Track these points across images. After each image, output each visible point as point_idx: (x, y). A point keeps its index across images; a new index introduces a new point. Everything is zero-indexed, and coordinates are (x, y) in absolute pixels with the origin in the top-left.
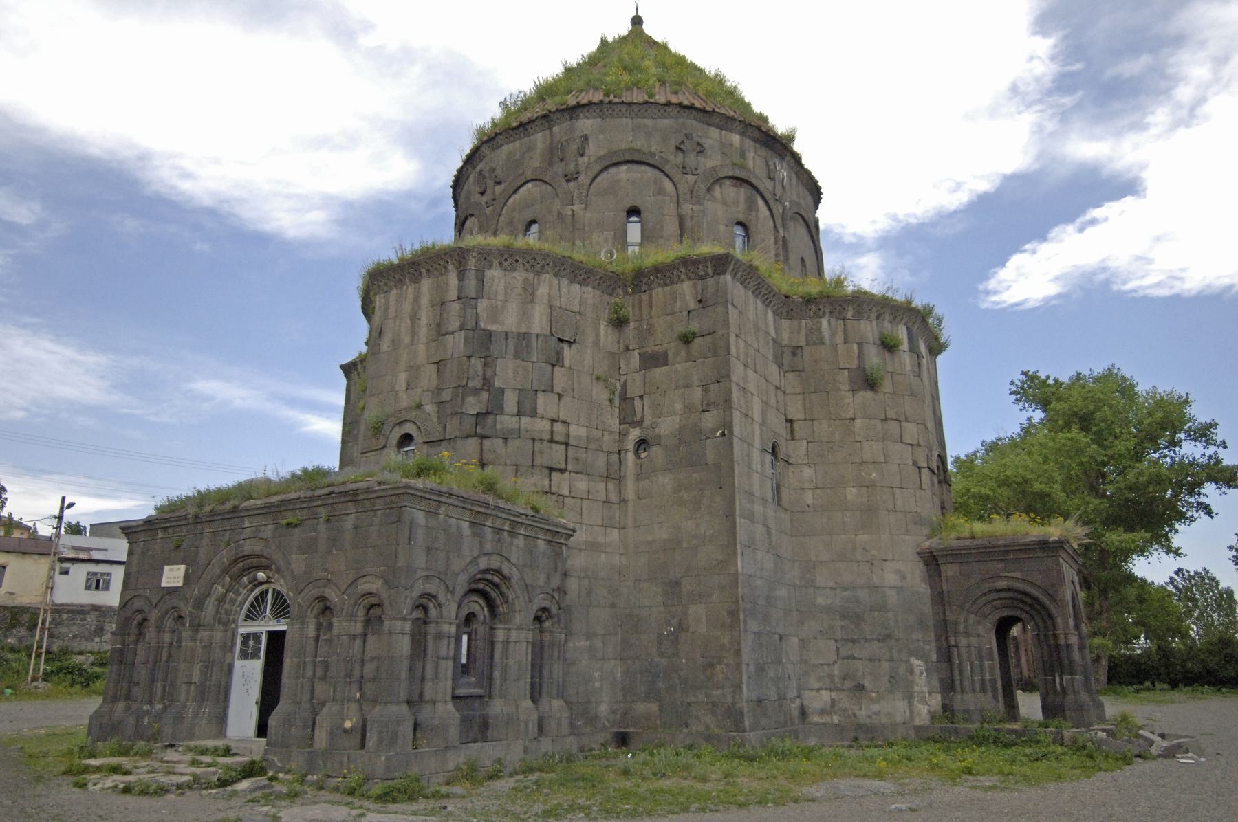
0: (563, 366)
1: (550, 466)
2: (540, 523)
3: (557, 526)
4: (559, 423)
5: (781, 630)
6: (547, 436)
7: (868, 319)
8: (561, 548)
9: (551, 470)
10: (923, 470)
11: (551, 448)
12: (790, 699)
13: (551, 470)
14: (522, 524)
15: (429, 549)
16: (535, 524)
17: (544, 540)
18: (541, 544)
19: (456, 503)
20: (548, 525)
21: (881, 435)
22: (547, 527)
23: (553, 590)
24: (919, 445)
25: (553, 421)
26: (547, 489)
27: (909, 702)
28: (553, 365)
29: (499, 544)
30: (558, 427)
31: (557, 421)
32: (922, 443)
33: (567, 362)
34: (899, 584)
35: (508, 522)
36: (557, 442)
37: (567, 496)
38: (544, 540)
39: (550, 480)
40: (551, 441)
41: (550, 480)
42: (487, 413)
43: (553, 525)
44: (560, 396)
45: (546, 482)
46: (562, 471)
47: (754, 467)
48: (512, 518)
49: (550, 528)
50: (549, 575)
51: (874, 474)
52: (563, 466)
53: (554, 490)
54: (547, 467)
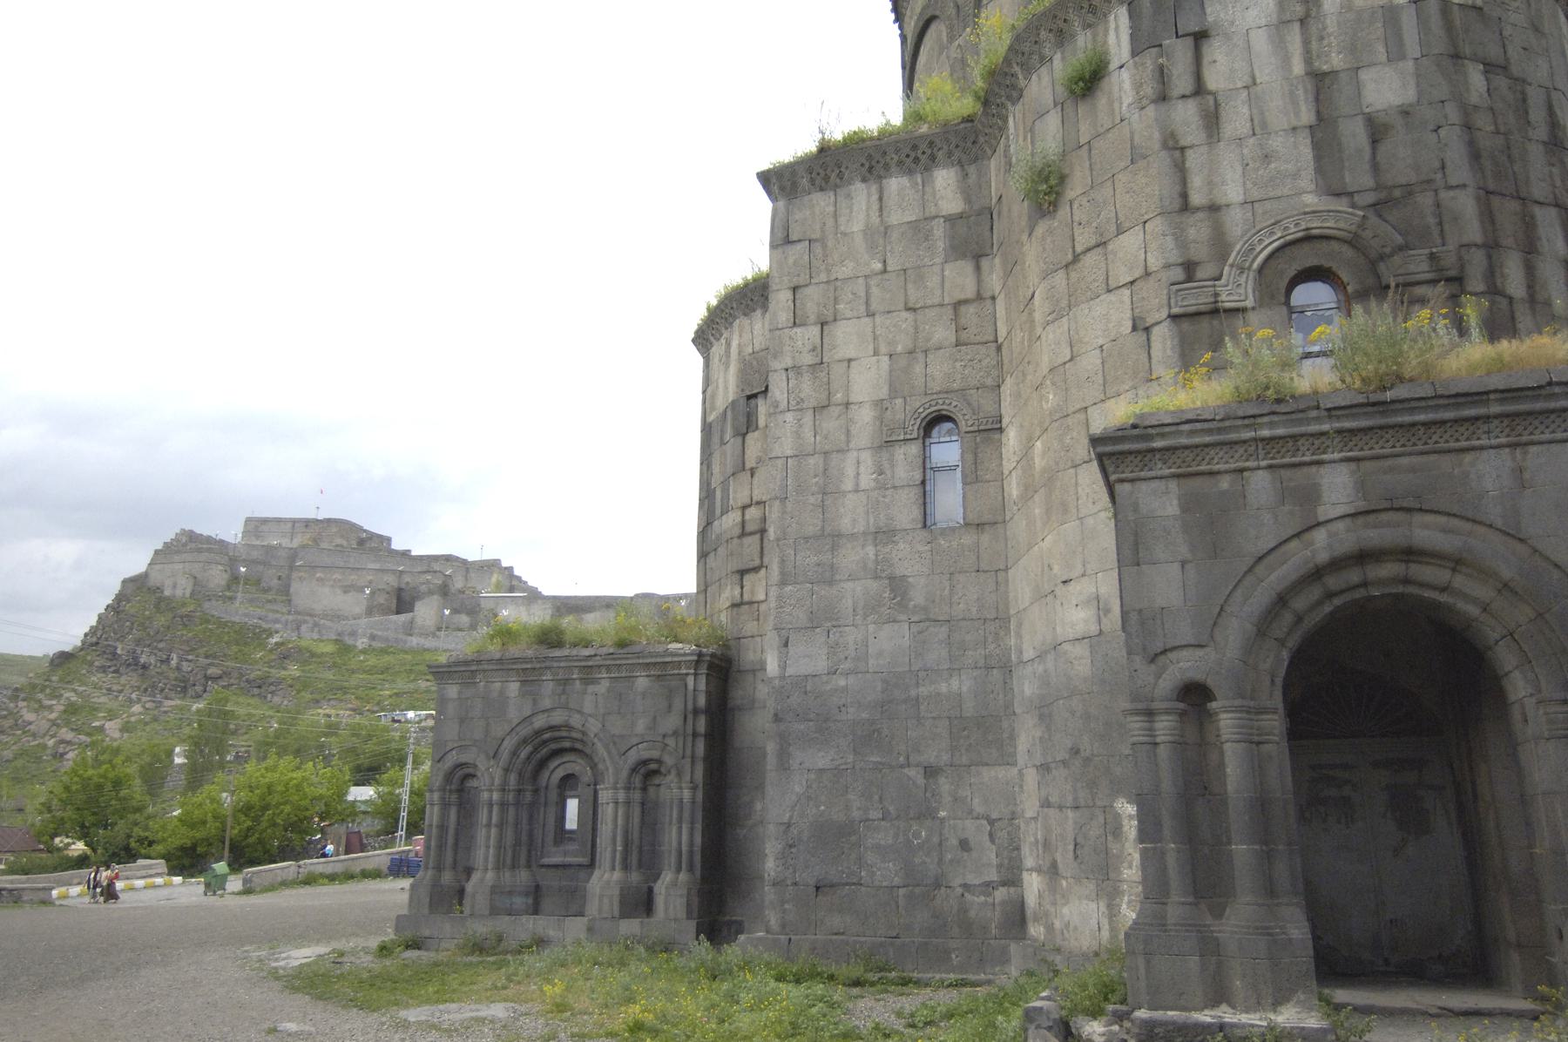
0: (757, 428)
1: (735, 569)
2: (627, 658)
3: (663, 656)
4: (753, 508)
5: (935, 753)
6: (737, 531)
7: (1043, 60)
8: (685, 680)
9: (742, 573)
10: (1156, 331)
11: (741, 545)
12: (965, 886)
13: (742, 573)
14: (599, 666)
15: (462, 721)
16: (618, 662)
17: (647, 676)
18: (642, 682)
19: (491, 667)
20: (643, 657)
21: (1064, 303)
22: (641, 661)
23: (664, 736)
24: (1147, 274)
25: (744, 508)
26: (738, 599)
27: (1110, 906)
28: (744, 435)
29: (563, 697)
30: (752, 513)
31: (750, 506)
32: (1154, 262)
33: (762, 422)
34: (1094, 629)
35: (576, 671)
36: (751, 534)
37: (762, 602)
38: (647, 676)
39: (742, 588)
40: (743, 534)
41: (742, 588)
42: (708, 524)
43: (652, 657)
44: (753, 472)
45: (737, 591)
46: (756, 569)
47: (848, 485)
48: (576, 664)
49: (648, 661)
50: (655, 718)
51: (1051, 397)
52: (757, 562)
53: (746, 598)
54: (738, 572)
